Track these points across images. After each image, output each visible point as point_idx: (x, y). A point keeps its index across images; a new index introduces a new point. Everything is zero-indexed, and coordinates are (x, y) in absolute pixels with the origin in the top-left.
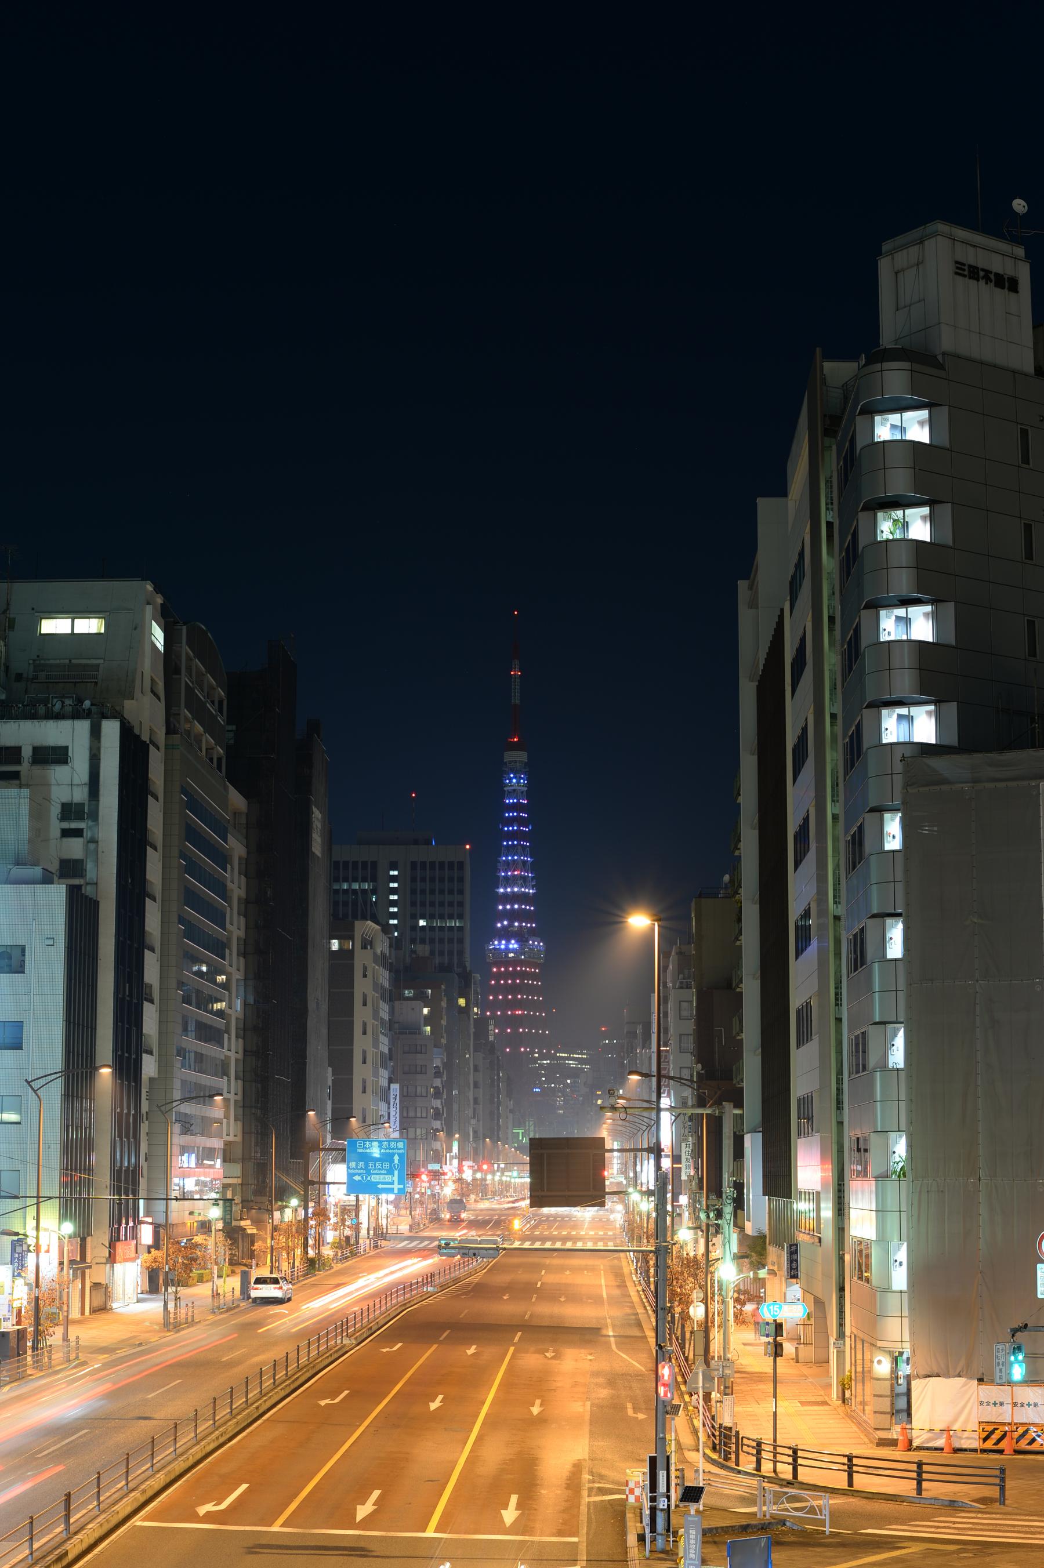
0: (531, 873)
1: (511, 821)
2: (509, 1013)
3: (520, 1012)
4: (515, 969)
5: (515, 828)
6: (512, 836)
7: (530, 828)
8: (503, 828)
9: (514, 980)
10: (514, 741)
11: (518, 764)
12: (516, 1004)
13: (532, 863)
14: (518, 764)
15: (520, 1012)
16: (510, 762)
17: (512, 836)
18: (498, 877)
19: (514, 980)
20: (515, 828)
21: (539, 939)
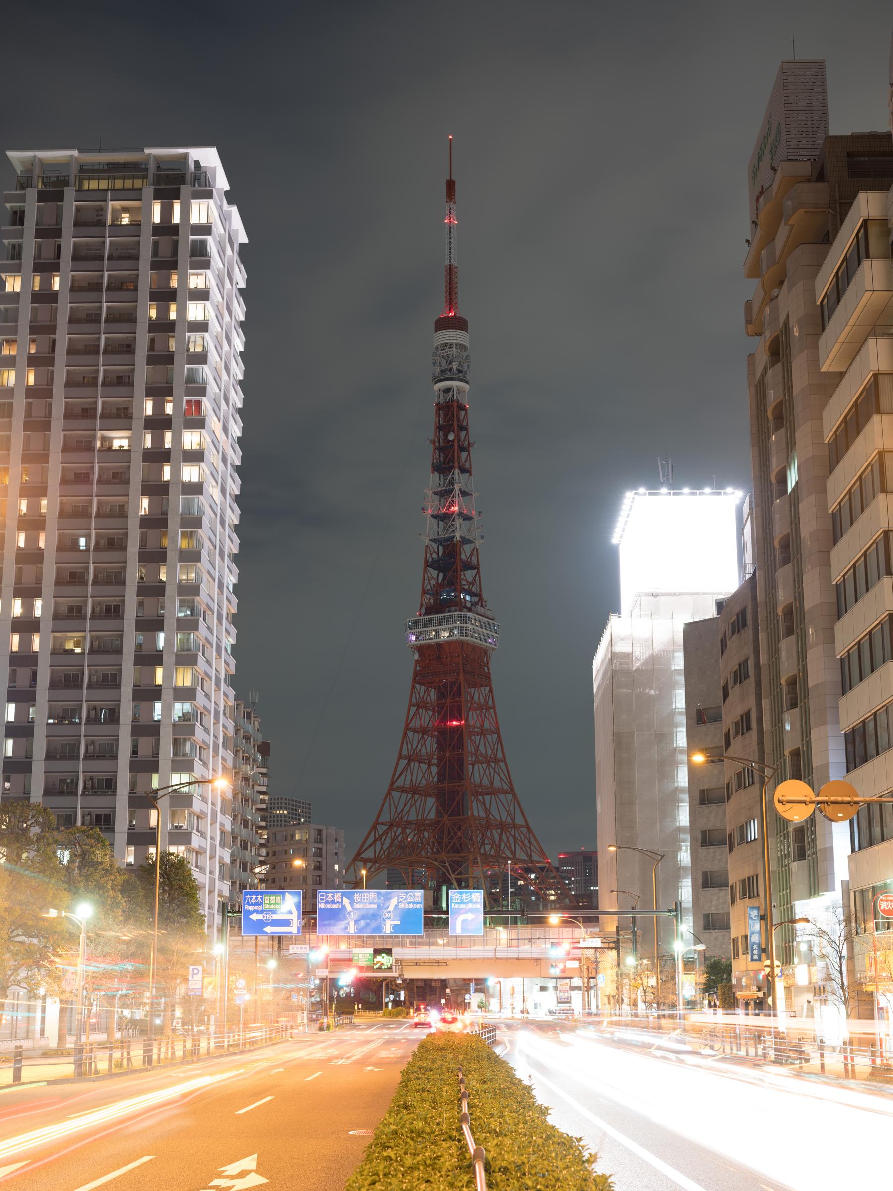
10: (448, 317)
11: (454, 349)
14: (454, 349)
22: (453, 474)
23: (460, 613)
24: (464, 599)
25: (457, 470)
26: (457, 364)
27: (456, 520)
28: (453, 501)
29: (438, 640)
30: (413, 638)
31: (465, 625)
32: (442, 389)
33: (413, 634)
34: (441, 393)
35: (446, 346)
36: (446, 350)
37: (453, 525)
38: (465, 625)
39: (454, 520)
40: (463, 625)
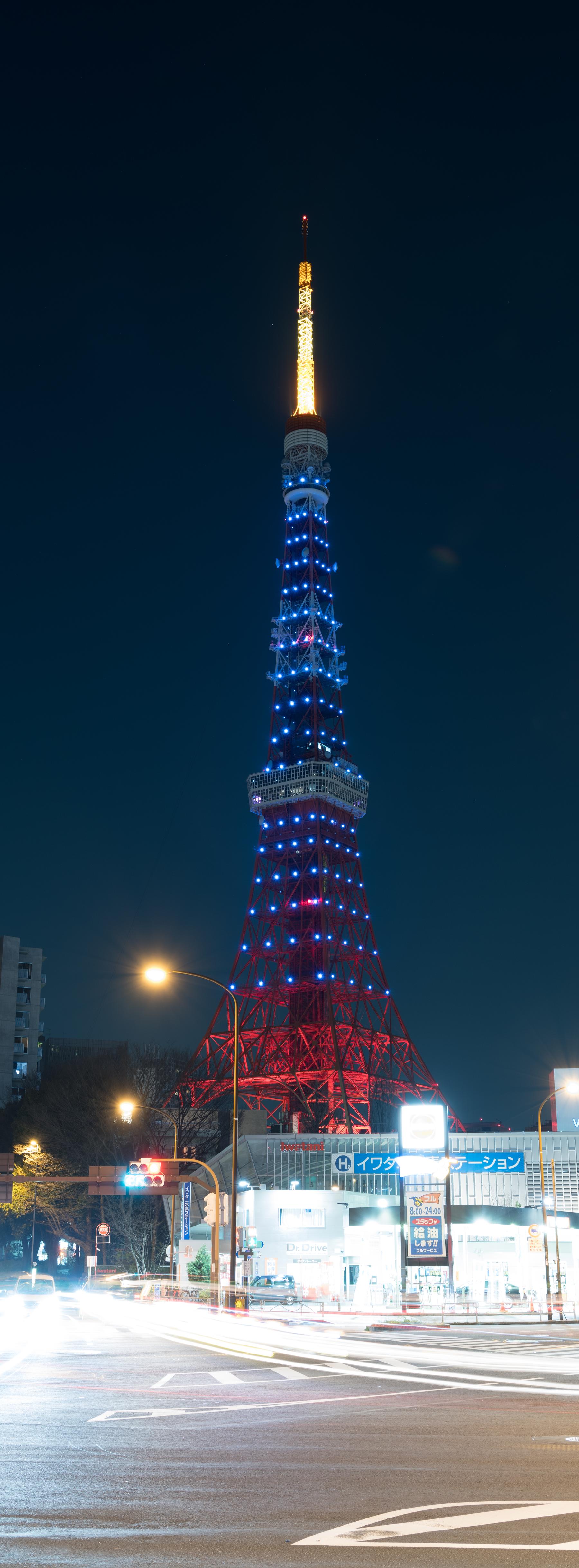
0: (338, 648)
1: (296, 551)
2: (294, 905)
3: (315, 902)
4: (305, 818)
5: (305, 561)
6: (297, 576)
7: (335, 568)
8: (282, 566)
9: (302, 840)
11: (309, 453)
12: (311, 887)
13: (339, 631)
14: (309, 453)
15: (315, 902)
16: (297, 449)
17: (297, 576)
18: (274, 654)
19: (302, 840)
20: (305, 561)
21: (356, 768)
22: (308, 597)
23: (316, 763)
24: (323, 749)
25: (312, 593)
26: (312, 469)
27: (312, 651)
28: (308, 631)
29: (288, 799)
30: (258, 799)
31: (322, 778)
32: (296, 499)
33: (258, 794)
34: (294, 506)
35: (299, 451)
36: (300, 455)
37: (308, 659)
38: (322, 778)
39: (309, 653)
40: (319, 778)
